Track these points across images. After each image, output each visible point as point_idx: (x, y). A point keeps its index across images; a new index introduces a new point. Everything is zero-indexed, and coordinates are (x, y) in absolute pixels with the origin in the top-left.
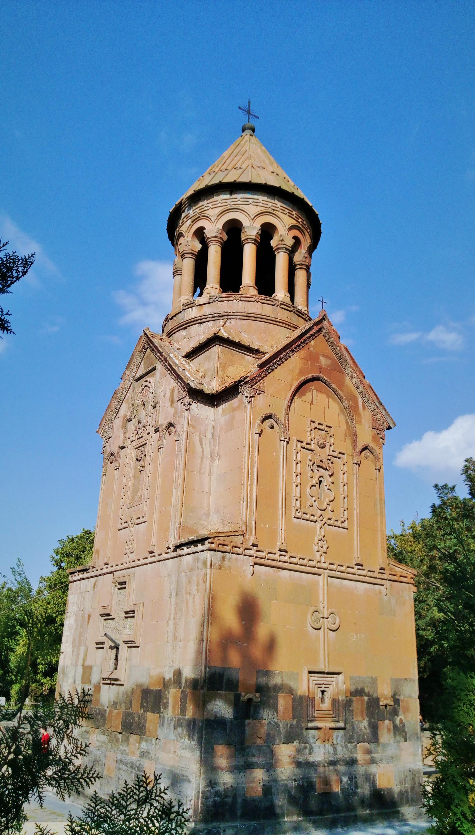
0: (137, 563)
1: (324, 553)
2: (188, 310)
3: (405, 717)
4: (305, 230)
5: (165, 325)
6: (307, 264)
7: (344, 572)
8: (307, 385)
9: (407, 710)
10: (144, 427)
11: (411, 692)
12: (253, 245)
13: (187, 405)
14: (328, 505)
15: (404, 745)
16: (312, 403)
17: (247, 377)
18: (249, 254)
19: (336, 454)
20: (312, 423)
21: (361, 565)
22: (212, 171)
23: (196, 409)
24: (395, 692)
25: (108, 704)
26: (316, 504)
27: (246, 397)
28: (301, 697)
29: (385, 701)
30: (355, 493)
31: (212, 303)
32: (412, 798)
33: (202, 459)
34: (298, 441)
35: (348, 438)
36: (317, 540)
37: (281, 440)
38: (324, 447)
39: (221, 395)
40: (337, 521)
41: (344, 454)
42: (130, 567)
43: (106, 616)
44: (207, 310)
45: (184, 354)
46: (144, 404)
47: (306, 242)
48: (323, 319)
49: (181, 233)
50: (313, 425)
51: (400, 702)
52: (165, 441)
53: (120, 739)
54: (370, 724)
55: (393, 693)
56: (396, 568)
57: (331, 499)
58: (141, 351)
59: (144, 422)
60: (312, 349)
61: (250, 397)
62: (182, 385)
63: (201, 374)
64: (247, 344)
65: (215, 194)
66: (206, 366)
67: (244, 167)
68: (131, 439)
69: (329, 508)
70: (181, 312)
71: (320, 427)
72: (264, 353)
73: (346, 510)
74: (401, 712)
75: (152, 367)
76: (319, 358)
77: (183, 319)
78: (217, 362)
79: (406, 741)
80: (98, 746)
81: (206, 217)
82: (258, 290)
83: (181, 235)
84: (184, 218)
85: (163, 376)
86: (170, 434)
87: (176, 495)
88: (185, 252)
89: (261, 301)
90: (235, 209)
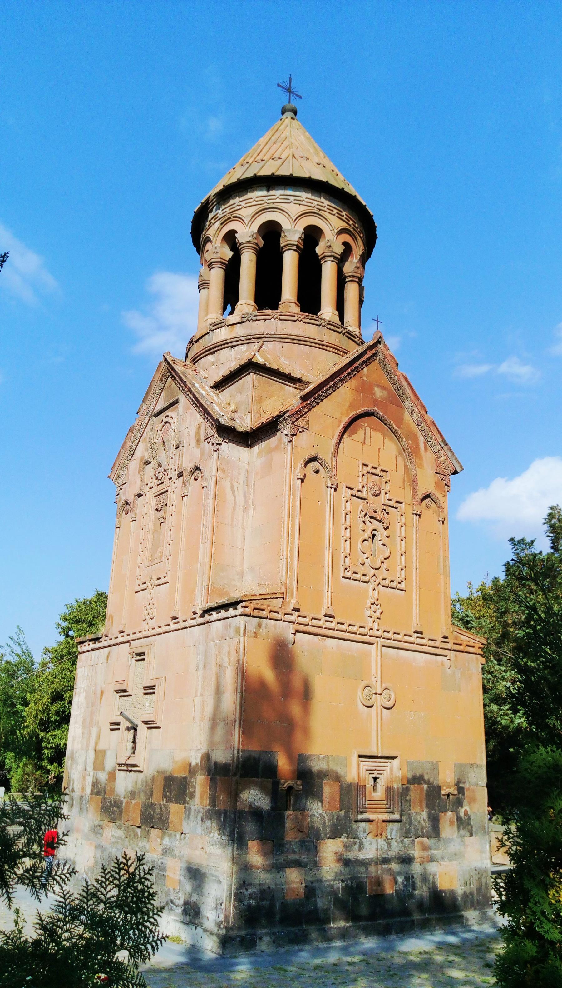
0: (158, 630)
1: (378, 618)
2: (217, 330)
3: (470, 808)
4: (357, 235)
5: (189, 349)
6: (359, 275)
7: (401, 641)
9: (473, 800)
10: (165, 471)
11: (478, 779)
12: (295, 252)
13: (215, 444)
14: (383, 563)
15: (469, 840)
16: (364, 443)
17: (287, 412)
18: (290, 262)
19: (392, 503)
20: (364, 467)
21: (421, 633)
22: (245, 162)
24: (459, 779)
25: (124, 794)
26: (368, 562)
27: (287, 435)
28: (350, 785)
30: (414, 549)
31: (245, 322)
32: (478, 900)
33: (234, 510)
34: (347, 487)
35: (407, 484)
36: (370, 604)
37: (328, 487)
38: (379, 495)
40: (392, 581)
41: (401, 503)
42: (149, 635)
43: (122, 692)
44: (240, 331)
45: (212, 384)
46: (164, 443)
47: (358, 249)
48: (378, 342)
49: (208, 237)
50: (366, 469)
51: (465, 791)
52: (190, 488)
53: (139, 834)
54: (430, 816)
56: (462, 636)
57: (387, 555)
58: (161, 380)
59: (164, 466)
60: (365, 378)
61: (291, 435)
62: (210, 421)
63: (232, 408)
64: (287, 372)
65: (249, 190)
66: (239, 398)
67: (284, 157)
68: (150, 485)
69: (384, 566)
70: (208, 333)
71: (374, 471)
72: (307, 383)
73: (404, 568)
74: (465, 802)
75: (174, 399)
76: (372, 389)
77: (210, 342)
78: (251, 393)
79: (471, 835)
80: (113, 843)
82: (300, 307)
83: (208, 240)
84: (212, 219)
85: (187, 410)
86: (196, 480)
87: (203, 551)
88: (212, 260)
89: (304, 320)
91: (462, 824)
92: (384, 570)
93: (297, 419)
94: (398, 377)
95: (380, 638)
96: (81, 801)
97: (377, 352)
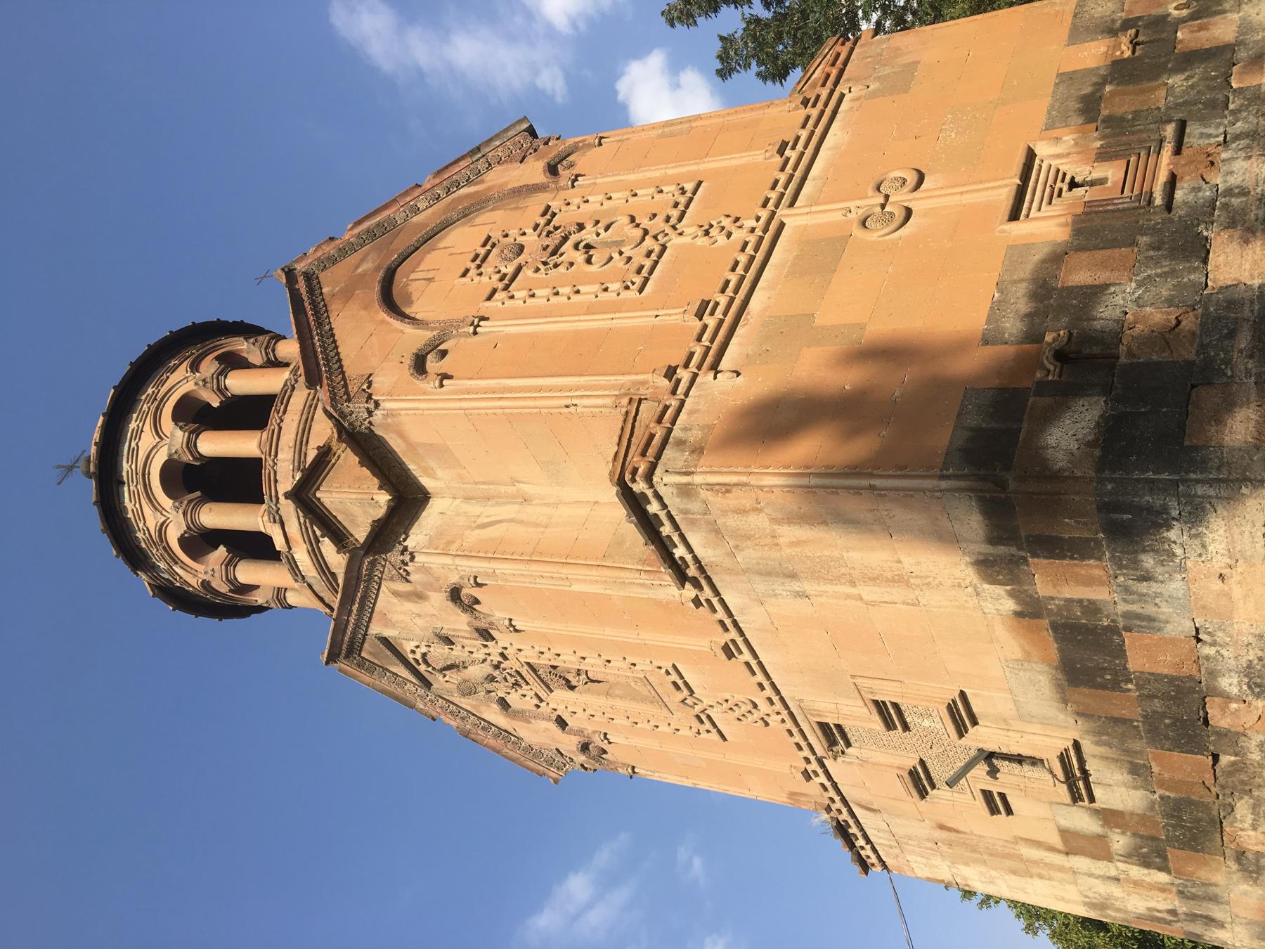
16: (430, 280)
19: (542, 221)
20: (470, 274)
24: (1102, 32)
27: (370, 413)
33: (522, 522)
37: (475, 333)
39: (393, 480)
50: (473, 272)
52: (498, 615)
53: (1233, 758)
57: (626, 220)
59: (487, 669)
69: (645, 223)
70: (310, 586)
81: (162, 529)
86: (477, 602)
90: (144, 475)
91: (1208, 8)
93: (347, 393)
96: (1193, 897)
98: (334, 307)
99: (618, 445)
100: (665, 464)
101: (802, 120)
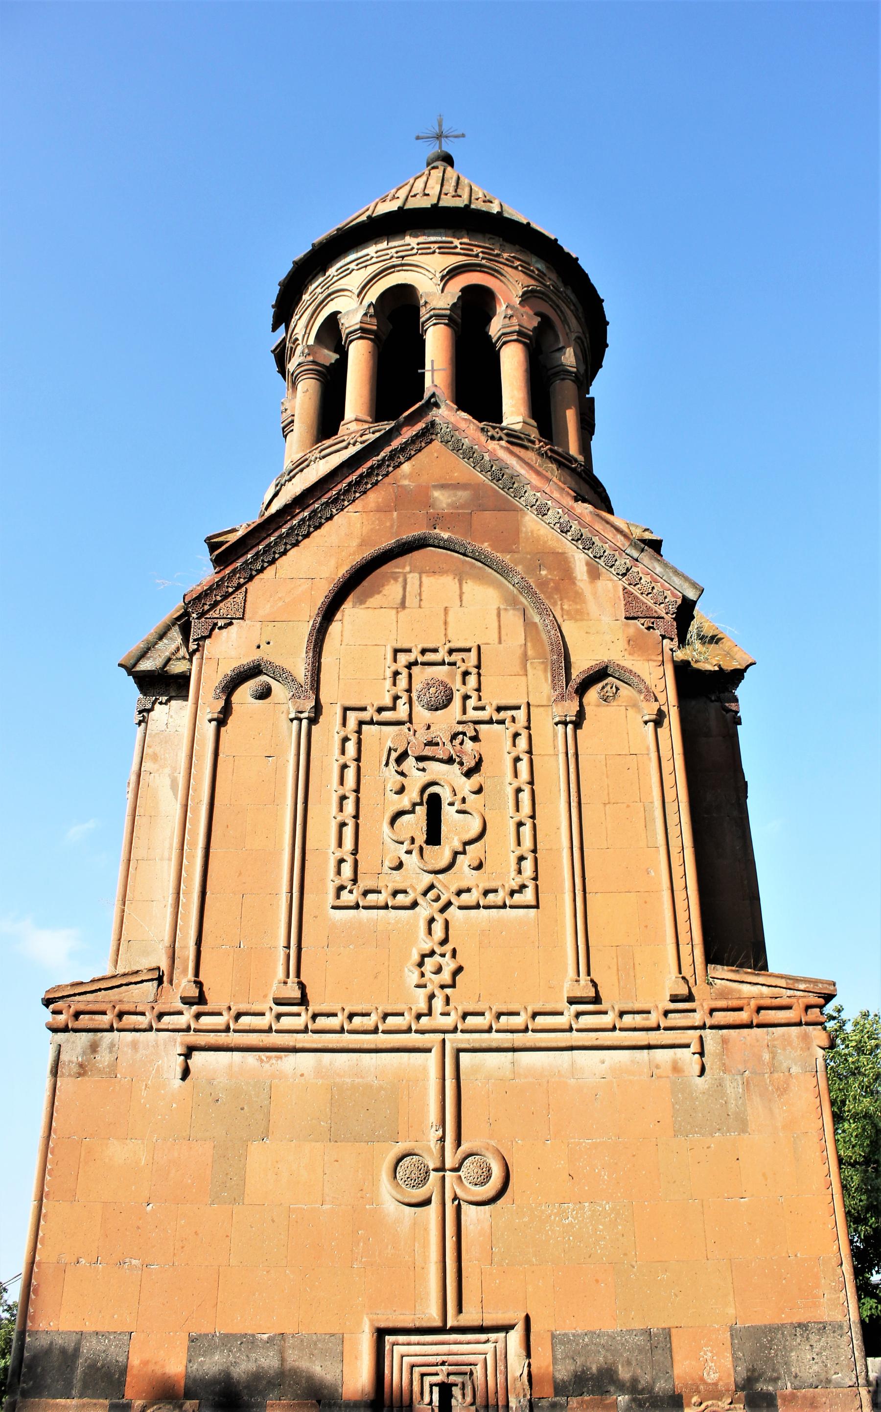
1: (443, 987)
8: (385, 569)
16: (403, 605)
20: (399, 655)
23: (164, 718)
24: (754, 1370)
29: (710, 1403)
34: (346, 709)
36: (416, 958)
37: (292, 720)
41: (518, 708)
50: (403, 659)
55: (744, 1375)
60: (406, 482)
71: (430, 657)
76: (428, 497)
92: (466, 869)
93: (216, 603)
94: (492, 453)
95: (455, 1030)
97: (433, 424)
98: (373, 498)
99: (93, 981)
100: (68, 1041)
101: (638, 1006)
